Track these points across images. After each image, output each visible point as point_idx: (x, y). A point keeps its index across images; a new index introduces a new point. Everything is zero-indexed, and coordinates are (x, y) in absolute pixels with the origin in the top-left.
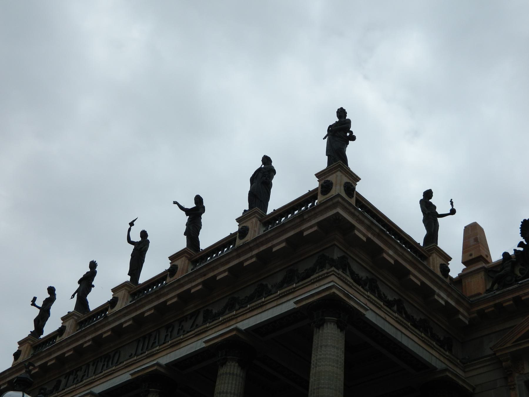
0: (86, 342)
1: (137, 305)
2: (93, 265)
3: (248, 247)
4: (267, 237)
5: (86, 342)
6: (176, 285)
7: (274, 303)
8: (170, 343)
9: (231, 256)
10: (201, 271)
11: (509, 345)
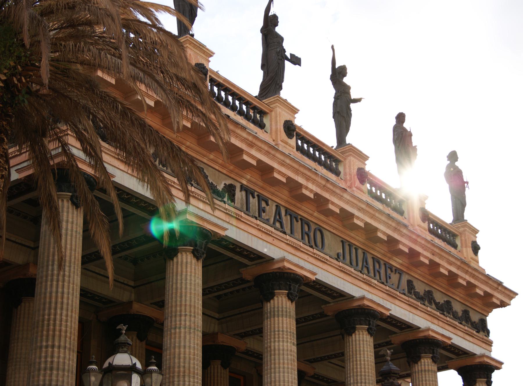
0: (307, 188)
3: (467, 269)
6: (414, 237)
8: (387, 288)
9: (456, 262)
10: (435, 249)
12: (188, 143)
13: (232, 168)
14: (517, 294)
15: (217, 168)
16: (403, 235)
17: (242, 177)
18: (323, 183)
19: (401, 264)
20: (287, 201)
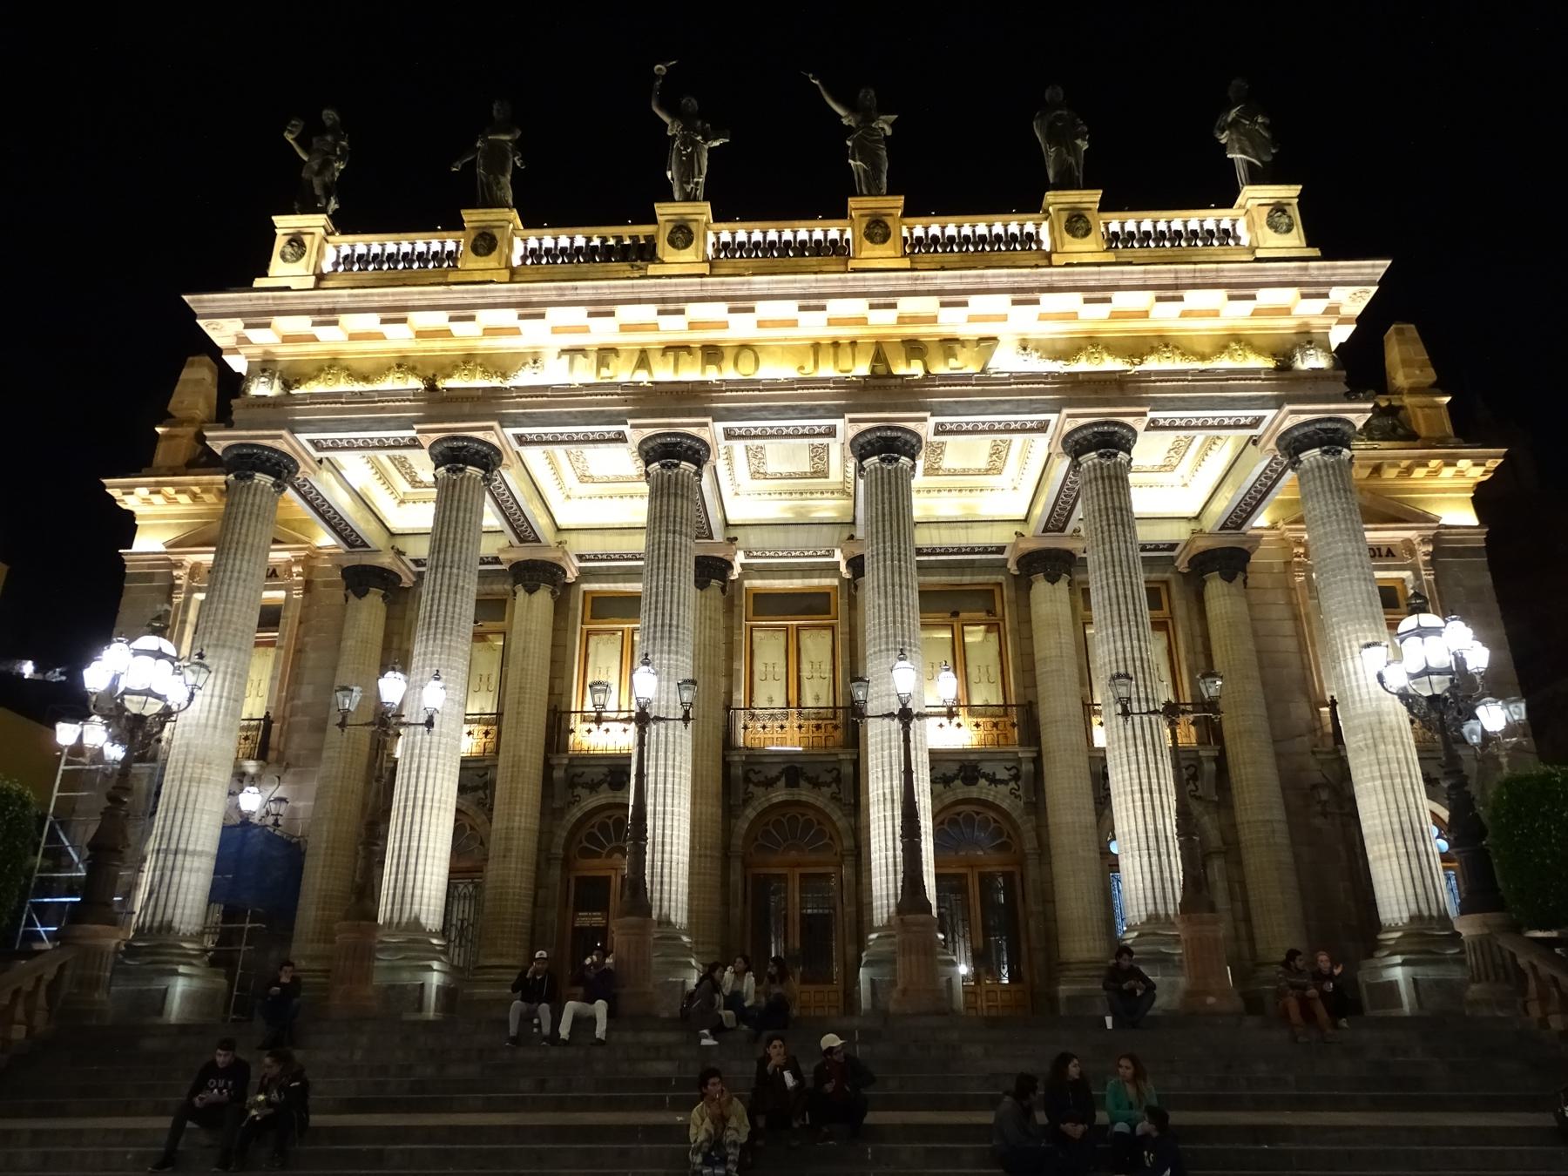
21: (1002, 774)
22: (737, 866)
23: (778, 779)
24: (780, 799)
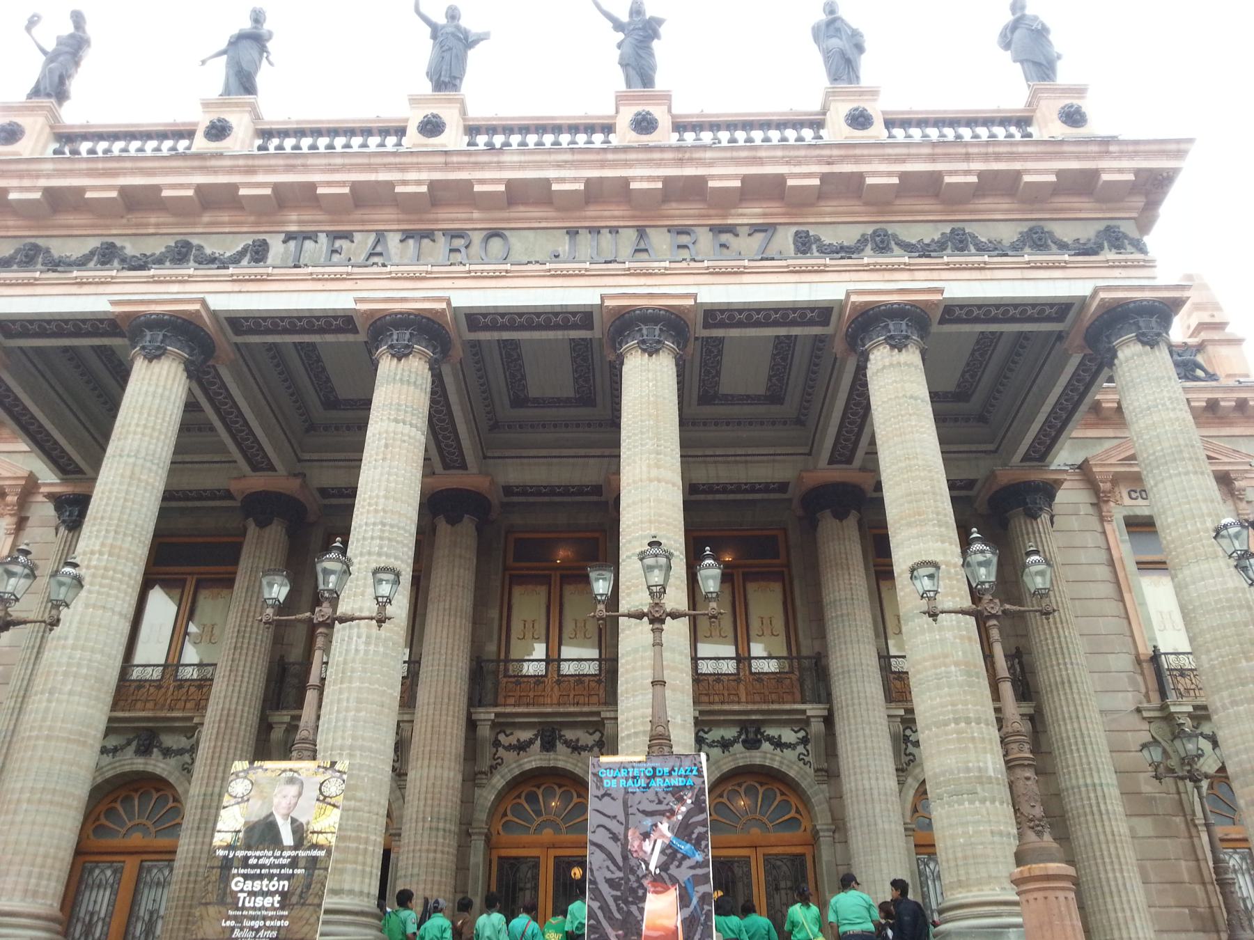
0: (405, 183)
1: (610, 156)
2: (258, 18)
3: (963, 150)
4: (1014, 149)
5: (405, 183)
7: (1018, 274)
11: (1113, 461)
12: (153, 220)
13: (252, 219)
14: (1190, 141)
15: (227, 230)
16: (712, 163)
17: (283, 223)
18: (441, 159)
19: (765, 215)
20: (399, 221)
21: (788, 736)
22: (479, 844)
23: (531, 742)
24: (534, 765)
